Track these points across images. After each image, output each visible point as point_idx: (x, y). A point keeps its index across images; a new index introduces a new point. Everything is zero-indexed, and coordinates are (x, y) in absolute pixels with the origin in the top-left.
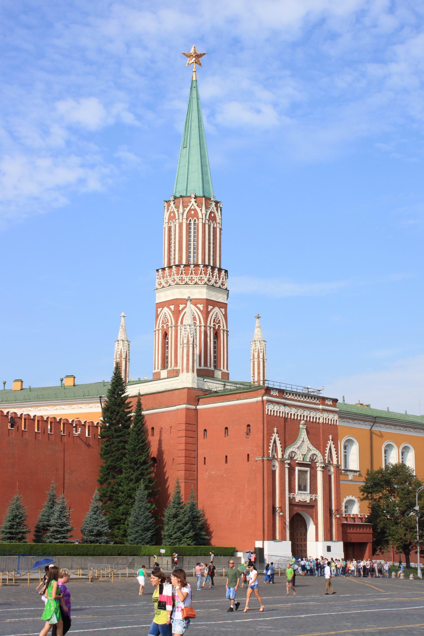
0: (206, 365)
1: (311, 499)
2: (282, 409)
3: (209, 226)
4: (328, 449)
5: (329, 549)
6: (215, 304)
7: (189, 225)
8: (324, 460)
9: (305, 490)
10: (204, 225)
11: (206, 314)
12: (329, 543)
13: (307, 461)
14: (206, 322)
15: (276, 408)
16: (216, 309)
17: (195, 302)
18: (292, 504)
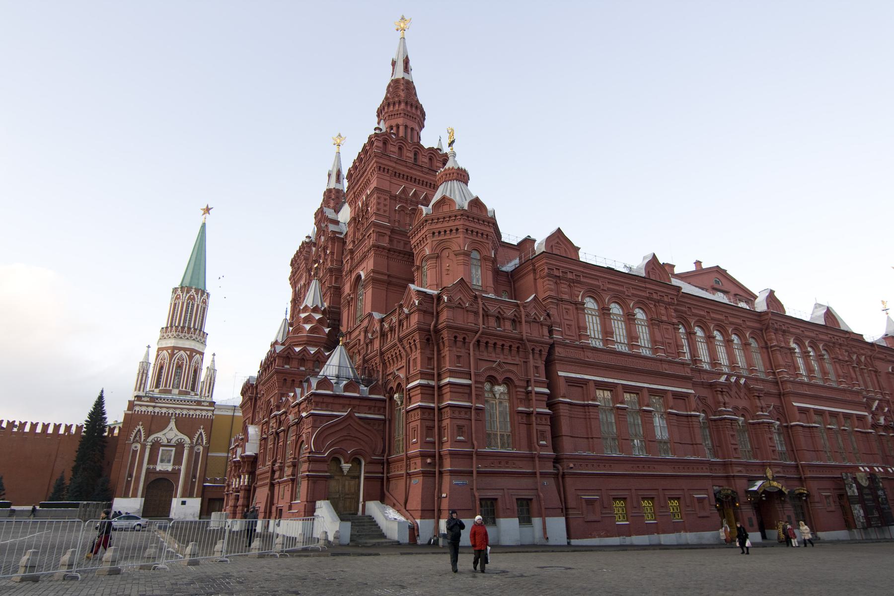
0: (166, 386)
1: (173, 469)
2: (150, 409)
3: (188, 304)
4: (197, 435)
5: (184, 503)
6: (180, 349)
7: (175, 304)
8: (192, 442)
9: (169, 461)
10: (183, 303)
11: (172, 355)
12: (184, 499)
13: (173, 443)
14: (171, 360)
15: (144, 409)
16: (182, 352)
17: (166, 349)
18: (148, 472)
